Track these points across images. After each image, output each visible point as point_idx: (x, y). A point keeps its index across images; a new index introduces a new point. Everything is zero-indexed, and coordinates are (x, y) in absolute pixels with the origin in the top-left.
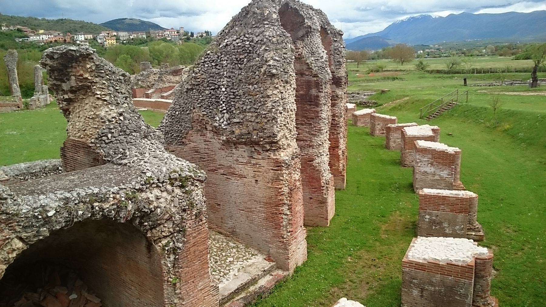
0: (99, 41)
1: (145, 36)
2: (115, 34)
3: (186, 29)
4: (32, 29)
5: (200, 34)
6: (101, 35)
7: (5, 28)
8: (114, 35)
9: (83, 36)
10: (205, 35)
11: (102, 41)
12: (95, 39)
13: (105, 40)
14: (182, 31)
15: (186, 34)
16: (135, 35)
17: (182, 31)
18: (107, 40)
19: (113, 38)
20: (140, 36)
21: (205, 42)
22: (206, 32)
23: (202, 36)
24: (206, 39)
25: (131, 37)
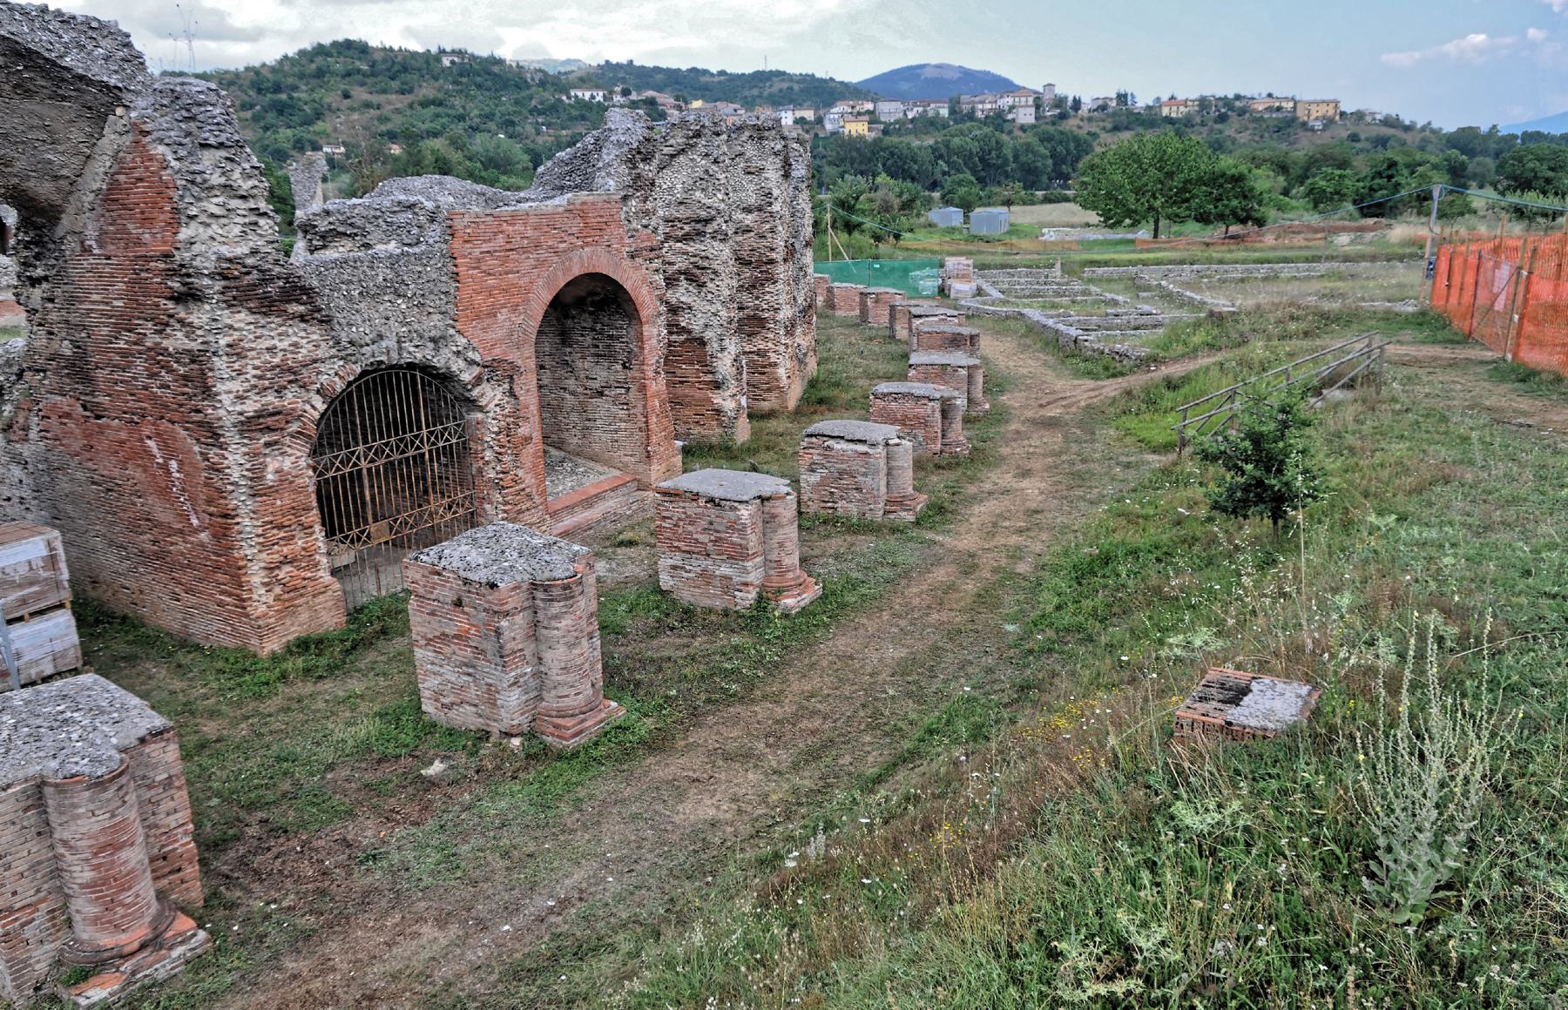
0: (829, 127)
1: (944, 112)
2: (869, 106)
3: (1060, 90)
4: (677, 99)
5: (1100, 102)
6: (835, 110)
7: (619, 98)
8: (868, 112)
9: (790, 114)
10: (1114, 104)
11: (836, 126)
12: (819, 121)
13: (842, 124)
14: (1048, 97)
15: (1059, 102)
16: (920, 109)
17: (1048, 97)
18: (847, 125)
19: (860, 118)
20: (931, 114)
21: (1109, 126)
23: (1103, 108)
24: (1114, 115)
25: (910, 116)
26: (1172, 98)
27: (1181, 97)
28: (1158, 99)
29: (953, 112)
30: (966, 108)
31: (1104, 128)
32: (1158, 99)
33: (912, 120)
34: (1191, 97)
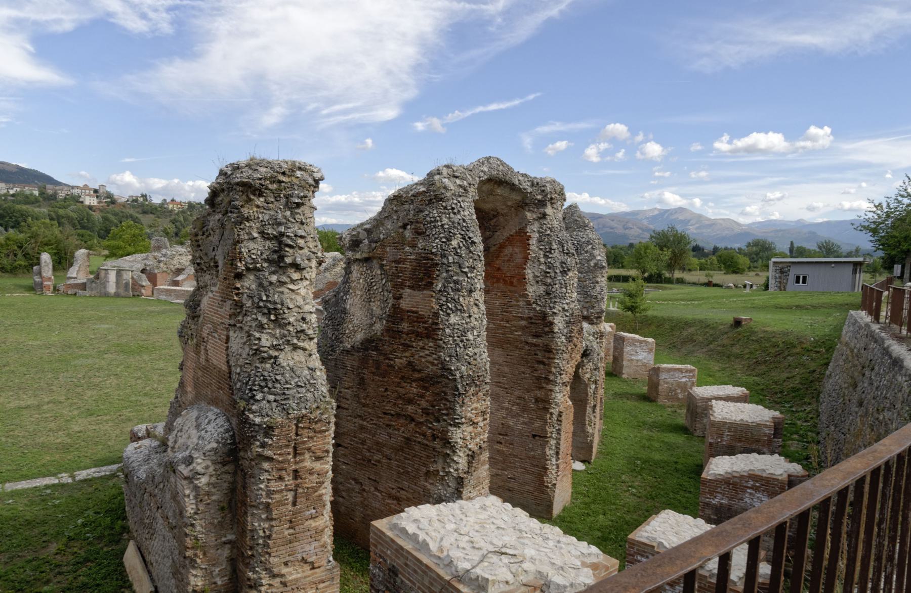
1: (36, 193)
3: (108, 189)
10: (141, 199)
20: (28, 192)
21: (141, 212)
22: (143, 196)
23: (136, 200)
25: (11, 192)
26: (173, 200)
27: (178, 200)
28: (165, 200)
29: (42, 193)
30: (50, 192)
31: (138, 212)
32: (165, 200)
33: (13, 195)
34: (183, 201)
